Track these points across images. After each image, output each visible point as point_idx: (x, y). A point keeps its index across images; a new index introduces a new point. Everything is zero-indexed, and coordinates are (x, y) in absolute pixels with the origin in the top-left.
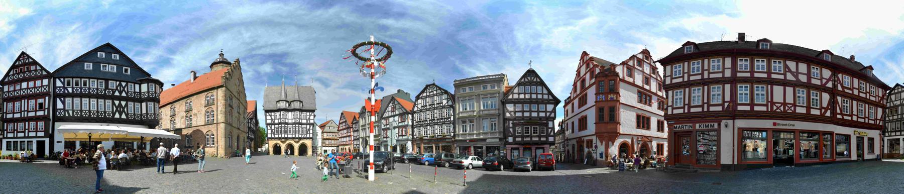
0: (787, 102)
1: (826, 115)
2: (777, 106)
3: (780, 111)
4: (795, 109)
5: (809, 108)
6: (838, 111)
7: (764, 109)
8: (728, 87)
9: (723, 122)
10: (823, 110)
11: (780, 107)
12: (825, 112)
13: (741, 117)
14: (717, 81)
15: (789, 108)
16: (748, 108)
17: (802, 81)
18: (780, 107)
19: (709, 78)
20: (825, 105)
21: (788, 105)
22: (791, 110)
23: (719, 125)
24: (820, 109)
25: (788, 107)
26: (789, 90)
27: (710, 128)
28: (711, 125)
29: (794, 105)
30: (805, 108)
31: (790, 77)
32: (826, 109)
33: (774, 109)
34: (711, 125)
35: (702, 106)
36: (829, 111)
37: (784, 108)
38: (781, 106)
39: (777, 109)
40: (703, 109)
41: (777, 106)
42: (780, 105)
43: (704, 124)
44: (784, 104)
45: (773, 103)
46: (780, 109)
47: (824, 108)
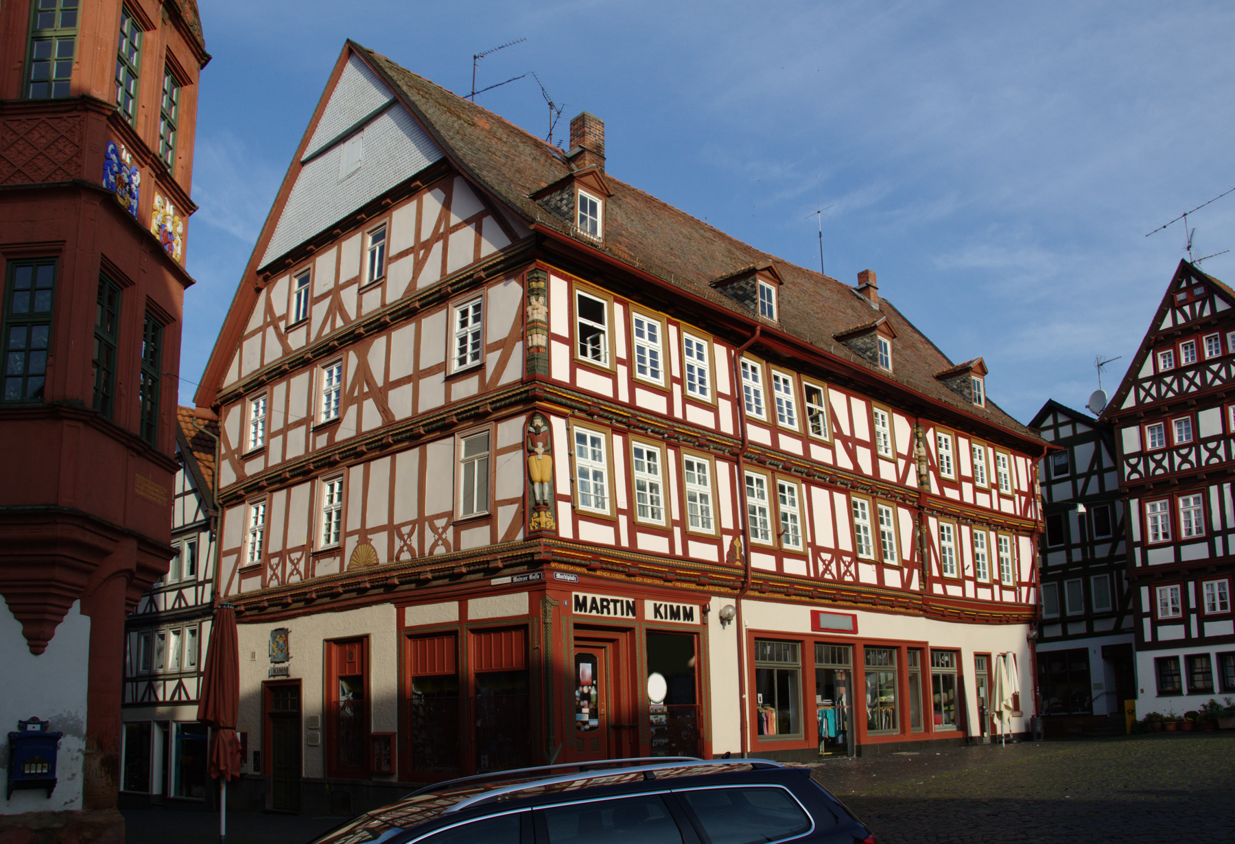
9: (718, 604)
23: (705, 611)
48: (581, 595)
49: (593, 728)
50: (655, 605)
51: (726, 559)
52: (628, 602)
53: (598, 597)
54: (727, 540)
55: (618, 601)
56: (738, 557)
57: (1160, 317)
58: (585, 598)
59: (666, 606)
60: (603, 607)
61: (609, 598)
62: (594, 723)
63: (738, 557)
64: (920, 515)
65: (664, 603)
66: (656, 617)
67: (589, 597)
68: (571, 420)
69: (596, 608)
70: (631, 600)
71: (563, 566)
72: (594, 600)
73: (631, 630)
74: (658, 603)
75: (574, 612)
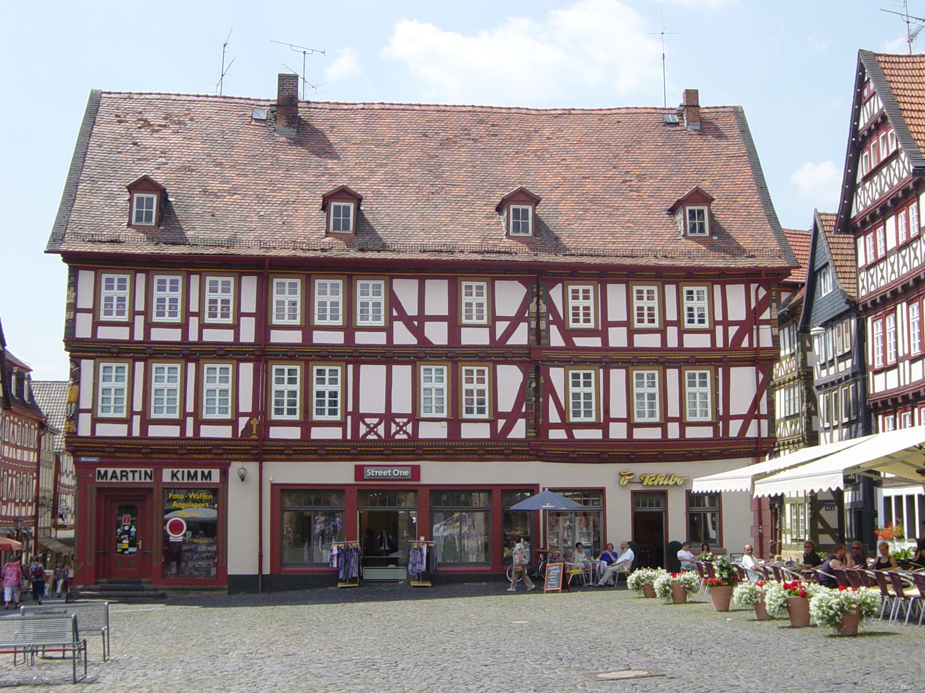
0: (393, 411)
1: (511, 436)
2: (368, 425)
3: (375, 437)
4: (416, 429)
5: (454, 423)
6: (554, 417)
7: (335, 433)
8: (247, 370)
9: (235, 468)
10: (501, 423)
11: (376, 426)
12: (508, 427)
13: (278, 457)
14: (220, 352)
15: (401, 428)
16: (294, 433)
17: (436, 342)
18: (376, 426)
19: (200, 342)
20: (506, 404)
21: (397, 420)
22: (405, 432)
23: (224, 475)
24: (493, 423)
25: (397, 424)
26: (402, 373)
27: (199, 480)
28: (203, 473)
29: (414, 418)
30: (445, 424)
31: (403, 336)
32: (511, 419)
33: (361, 434)
34: (203, 473)
35: (181, 423)
36: (521, 424)
37: (388, 429)
38: (379, 423)
39: (368, 433)
40: (183, 431)
41: (368, 425)
42: (376, 421)
43: (186, 470)
44: (388, 417)
45: (358, 417)
46: (376, 433)
47: (503, 415)
48: (103, 470)
49: (130, 553)
50: (173, 472)
51: (240, 435)
52: (146, 472)
53: (118, 470)
54: (243, 422)
55: (136, 471)
56: (254, 432)
57: (856, 116)
58: (106, 472)
59: (183, 472)
60: (122, 476)
61: (128, 470)
62: (133, 550)
63: (254, 432)
64: (537, 369)
65: (181, 470)
66: (172, 479)
67: (110, 471)
68: (98, 360)
69: (116, 477)
70: (149, 470)
71: (86, 453)
72: (114, 472)
73: (151, 490)
74: (175, 470)
75: (97, 481)
